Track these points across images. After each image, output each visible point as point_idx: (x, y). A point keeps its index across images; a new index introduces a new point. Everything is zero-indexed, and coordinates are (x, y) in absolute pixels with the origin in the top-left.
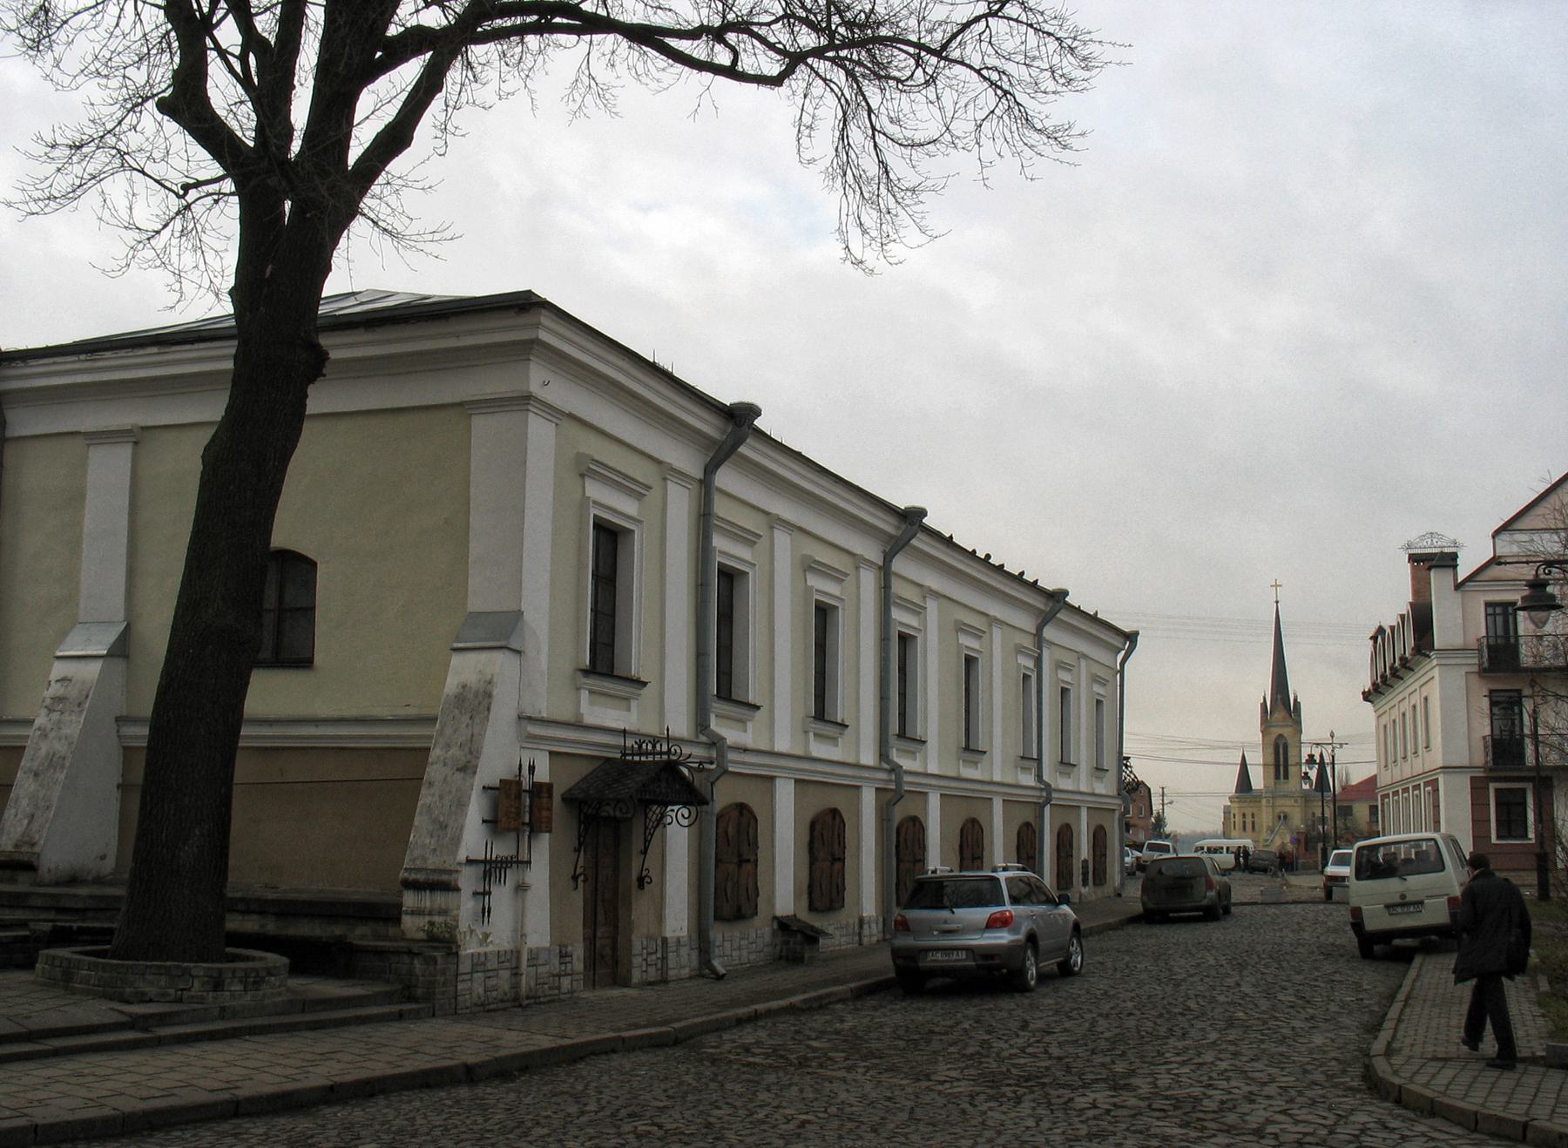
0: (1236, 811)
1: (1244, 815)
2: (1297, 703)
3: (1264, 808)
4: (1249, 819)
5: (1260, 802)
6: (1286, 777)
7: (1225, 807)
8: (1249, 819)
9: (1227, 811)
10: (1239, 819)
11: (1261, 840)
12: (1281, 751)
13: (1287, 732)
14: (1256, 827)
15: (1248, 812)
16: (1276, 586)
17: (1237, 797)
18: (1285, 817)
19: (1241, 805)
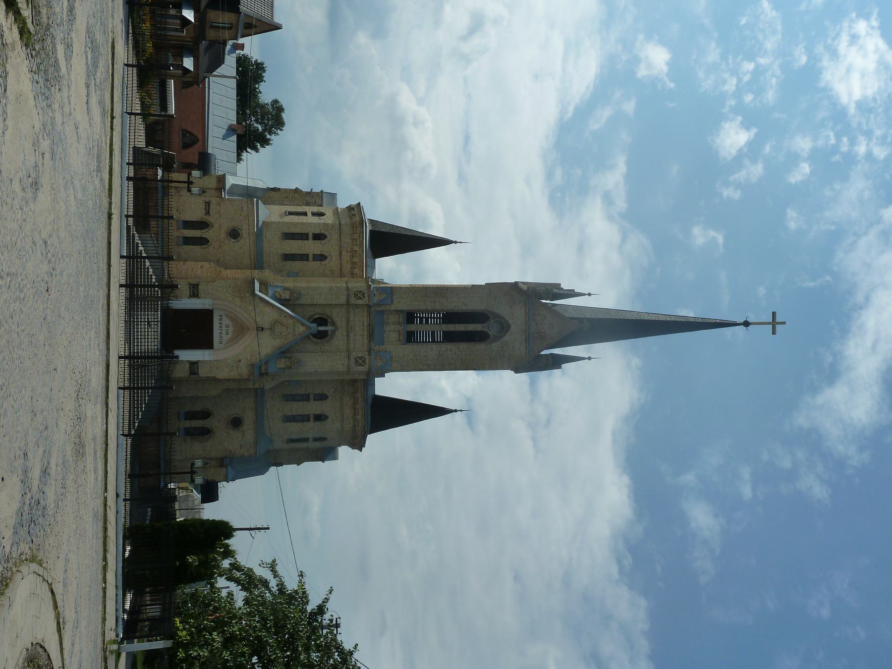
0: (329, 219)
1: (318, 237)
2: (556, 362)
3: (341, 283)
4: (311, 247)
5: (353, 275)
7: (333, 196)
8: (311, 247)
9: (315, 198)
11: (267, 274)
12: (471, 327)
13: (515, 339)
14: (297, 265)
15: (328, 247)
16: (774, 323)
17: (362, 222)
18: (322, 335)
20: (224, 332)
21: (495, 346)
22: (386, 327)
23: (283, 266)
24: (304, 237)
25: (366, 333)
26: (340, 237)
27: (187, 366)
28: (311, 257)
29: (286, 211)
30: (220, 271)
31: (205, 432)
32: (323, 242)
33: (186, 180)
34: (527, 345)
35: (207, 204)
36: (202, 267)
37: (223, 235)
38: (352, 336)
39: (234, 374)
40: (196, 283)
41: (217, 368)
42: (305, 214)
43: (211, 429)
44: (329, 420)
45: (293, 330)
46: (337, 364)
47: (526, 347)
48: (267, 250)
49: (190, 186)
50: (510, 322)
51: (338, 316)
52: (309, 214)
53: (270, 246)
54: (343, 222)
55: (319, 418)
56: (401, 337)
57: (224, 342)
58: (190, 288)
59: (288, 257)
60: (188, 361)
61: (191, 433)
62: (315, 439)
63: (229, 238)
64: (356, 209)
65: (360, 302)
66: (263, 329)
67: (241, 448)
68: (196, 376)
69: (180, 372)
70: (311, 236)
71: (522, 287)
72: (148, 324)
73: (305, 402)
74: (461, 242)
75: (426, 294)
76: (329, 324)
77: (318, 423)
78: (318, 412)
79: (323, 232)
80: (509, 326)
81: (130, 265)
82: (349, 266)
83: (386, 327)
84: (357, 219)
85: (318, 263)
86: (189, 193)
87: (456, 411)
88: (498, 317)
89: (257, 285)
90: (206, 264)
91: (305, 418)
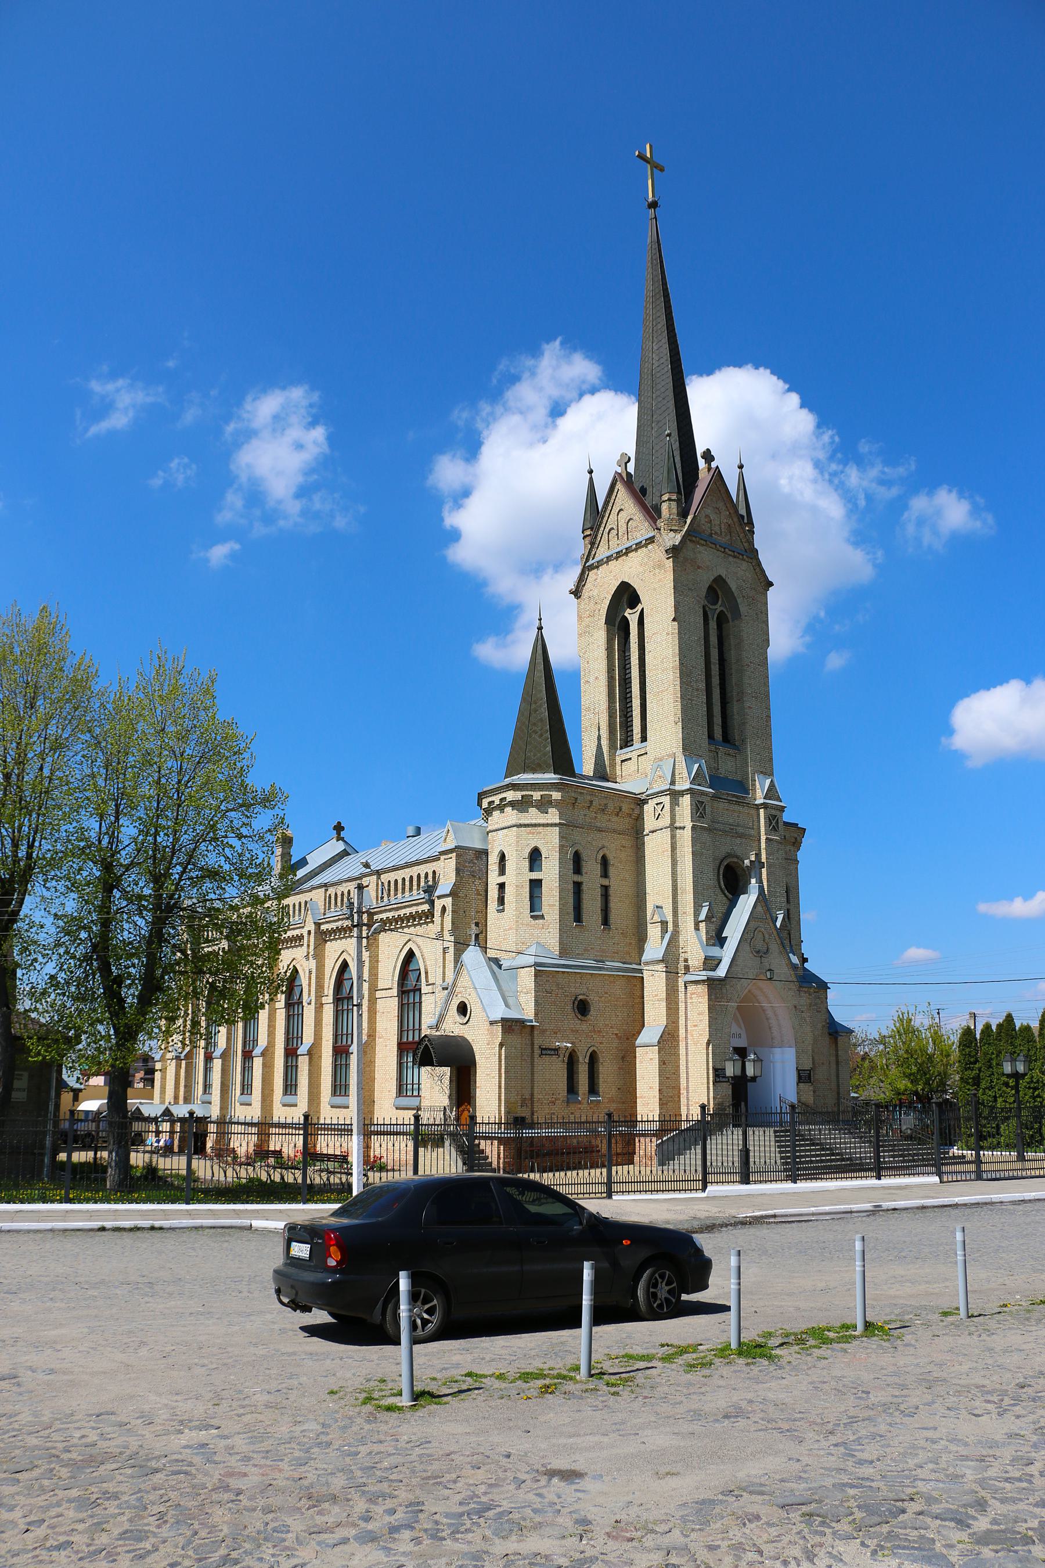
21: (743, 609)
25: (736, 807)
28: (605, 882)
29: (532, 917)
32: (584, 856)
36: (664, 1063)
37: (584, 1027)
38: (740, 830)
42: (535, 885)
47: (743, 560)
50: (716, 575)
52: (535, 875)
54: (557, 821)
56: (731, 751)
57: (739, 1031)
58: (719, 1082)
64: (524, 793)
70: (577, 878)
75: (689, 699)
81: (814, 1174)
82: (615, 819)
84: (556, 795)
85: (612, 871)
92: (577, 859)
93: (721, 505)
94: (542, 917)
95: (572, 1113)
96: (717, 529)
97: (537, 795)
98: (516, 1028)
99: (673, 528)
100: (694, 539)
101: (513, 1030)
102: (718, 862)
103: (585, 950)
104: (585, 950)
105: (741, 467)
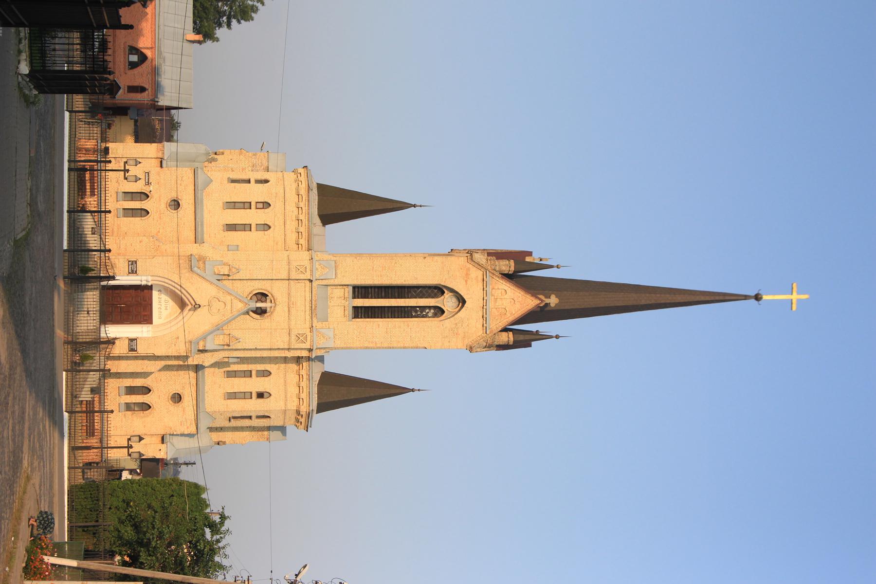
4: (253, 217)
6: (359, 313)
8: (253, 217)
10: (254, 193)
18: (261, 312)
19: (292, 197)
20: (163, 307)
22: (330, 302)
23: (224, 236)
24: (246, 205)
25: (308, 308)
26: (284, 205)
27: (127, 342)
30: (159, 246)
31: (146, 407)
33: (123, 169)
34: (485, 322)
35: (147, 175)
36: (140, 242)
37: (163, 206)
38: (293, 311)
39: (172, 352)
40: (135, 260)
41: (155, 345)
42: (249, 181)
43: (151, 405)
44: (271, 397)
45: (231, 306)
46: (277, 341)
48: (208, 221)
49: (127, 174)
51: (277, 291)
52: (252, 181)
53: (211, 216)
55: (260, 395)
56: (347, 312)
59: (231, 227)
60: (128, 338)
61: (129, 407)
62: (258, 417)
63: (169, 209)
65: (302, 277)
66: (200, 306)
67: (181, 425)
68: (135, 352)
69: (120, 349)
71: (479, 260)
72: (88, 313)
73: (247, 379)
74: (421, 206)
76: (268, 300)
77: (260, 400)
78: (261, 390)
79: (266, 200)
80: (466, 302)
82: (295, 235)
83: (330, 302)
86: (126, 180)
87: (413, 390)
88: (452, 290)
89: (194, 262)
90: (145, 239)
91: (246, 395)
92: (266, 205)
93: (518, 306)
94: (228, 182)
95: (111, 196)
96: (499, 303)
97: (303, 178)
98: (160, 155)
99: (489, 263)
100: (485, 277)
101: (159, 152)
102: (269, 289)
103: (210, 211)
104: (210, 211)
105: (557, 337)
